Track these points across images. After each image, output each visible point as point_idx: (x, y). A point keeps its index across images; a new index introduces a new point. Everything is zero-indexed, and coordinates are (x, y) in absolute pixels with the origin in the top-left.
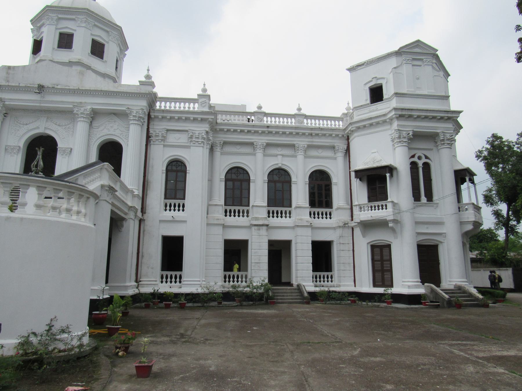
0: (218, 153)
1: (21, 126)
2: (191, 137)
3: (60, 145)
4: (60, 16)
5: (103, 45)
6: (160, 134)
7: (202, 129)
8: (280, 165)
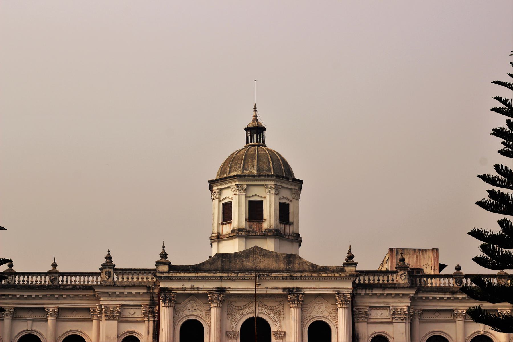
0: (417, 324)
2: (394, 314)
3: (274, 328)
4: (249, 183)
5: (287, 205)
6: (363, 311)
7: (403, 304)
8: (482, 333)
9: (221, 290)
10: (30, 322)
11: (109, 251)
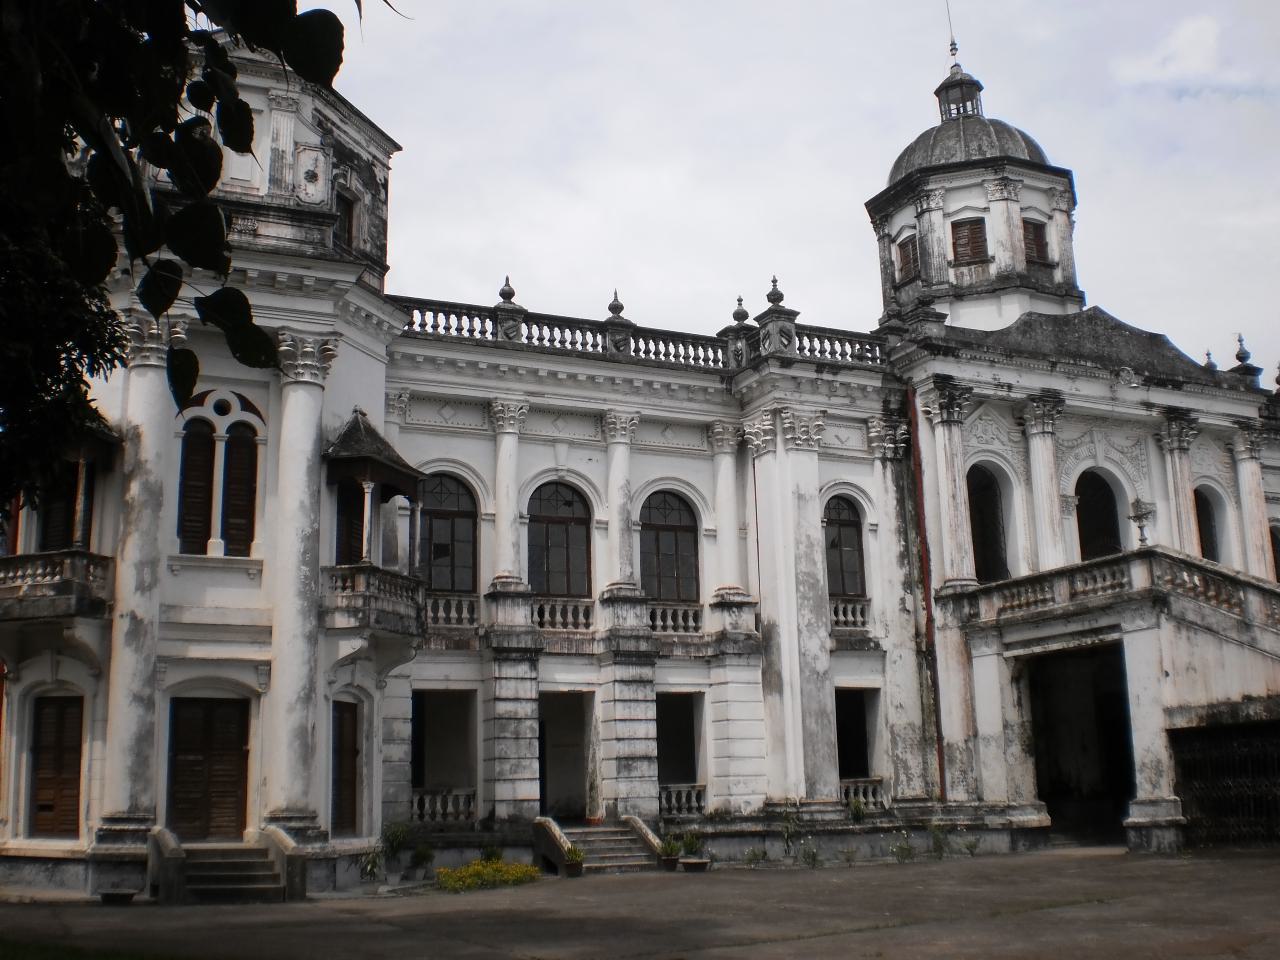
1: (1064, 449)
9: (1051, 400)
10: (562, 449)
11: (774, 281)
